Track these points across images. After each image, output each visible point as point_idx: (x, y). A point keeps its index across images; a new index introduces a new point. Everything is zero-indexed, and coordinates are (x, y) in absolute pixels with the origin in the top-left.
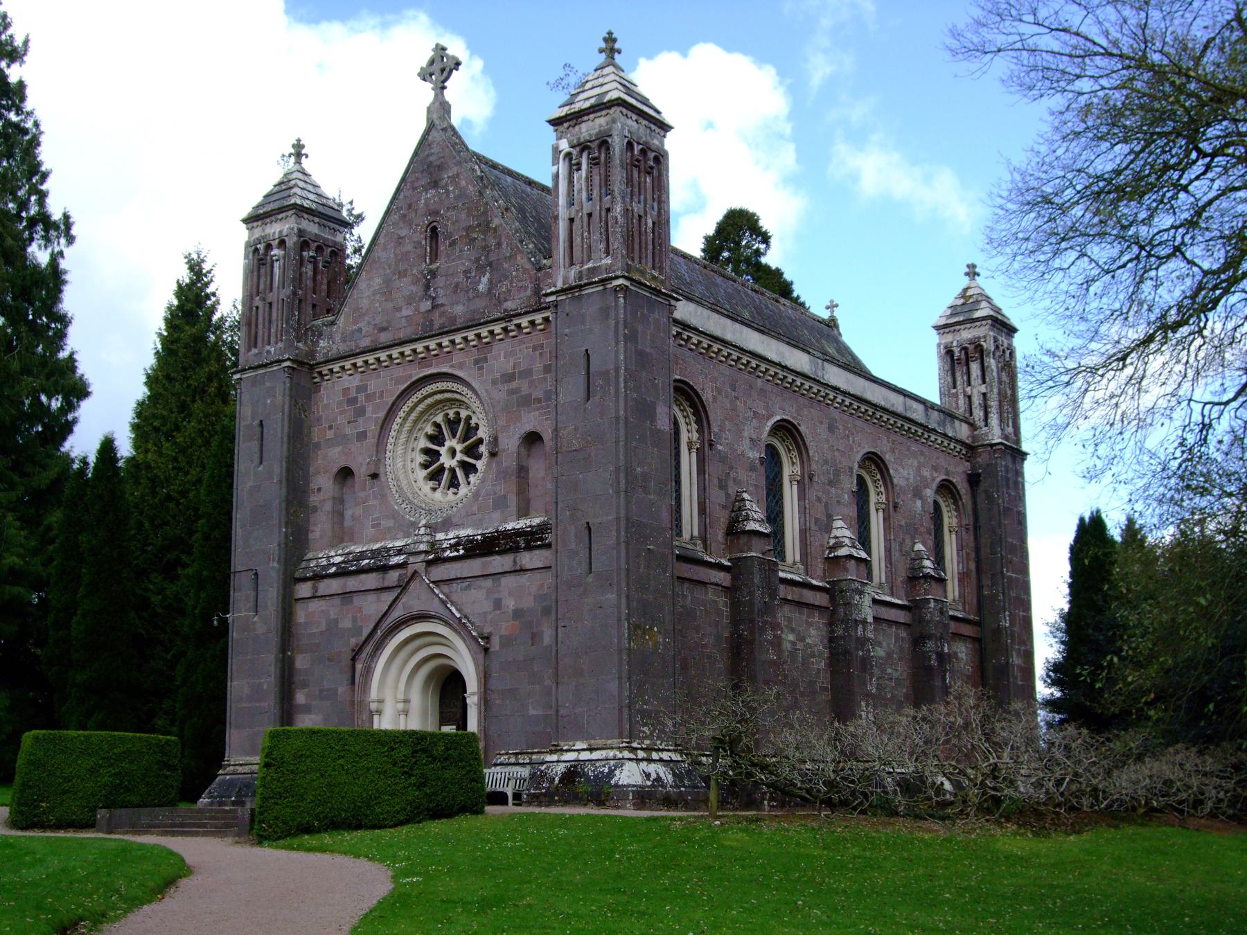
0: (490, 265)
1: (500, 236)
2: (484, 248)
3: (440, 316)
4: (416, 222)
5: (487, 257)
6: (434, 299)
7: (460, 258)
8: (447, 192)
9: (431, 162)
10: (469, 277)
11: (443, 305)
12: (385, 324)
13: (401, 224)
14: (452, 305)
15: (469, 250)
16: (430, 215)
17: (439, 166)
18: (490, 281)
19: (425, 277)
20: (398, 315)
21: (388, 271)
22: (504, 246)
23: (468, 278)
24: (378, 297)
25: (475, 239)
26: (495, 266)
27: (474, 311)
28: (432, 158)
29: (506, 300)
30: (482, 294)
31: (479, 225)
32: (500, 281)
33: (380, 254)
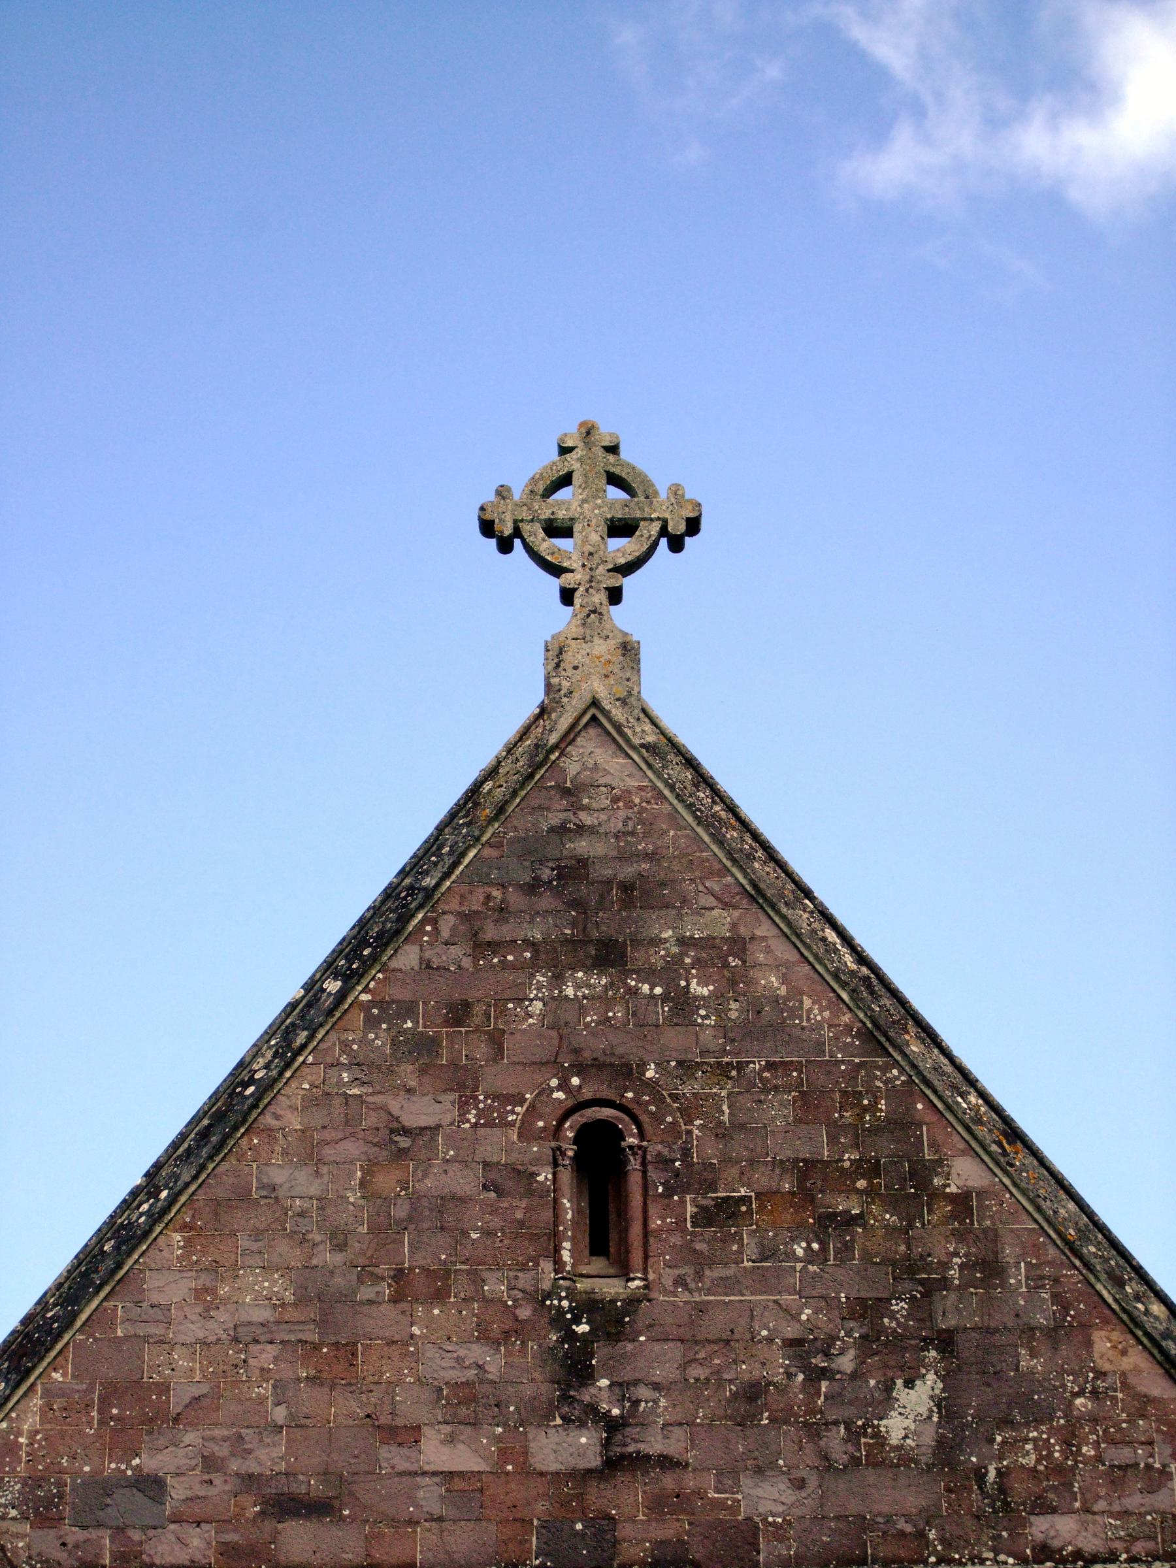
0: (946, 1342)
1: (992, 1236)
2: (909, 1268)
3: (658, 1505)
4: (496, 1078)
5: (922, 1306)
6: (613, 1426)
7: (763, 1281)
8: (682, 1004)
9: (582, 863)
10: (824, 1373)
11: (666, 1462)
12: (315, 1486)
13: (408, 1073)
14: (729, 1474)
15: (819, 1258)
16: (579, 1068)
17: (626, 888)
18: (947, 1407)
19: (558, 1320)
20: (392, 1457)
21: (327, 1257)
22: (1018, 1277)
23: (816, 1375)
24: (265, 1355)
25: (850, 1221)
26: (967, 1347)
27: (862, 1524)
28: (581, 846)
29: (1043, 1507)
30: (906, 1459)
31: (871, 1169)
32: (1006, 1422)
33: (278, 1176)
